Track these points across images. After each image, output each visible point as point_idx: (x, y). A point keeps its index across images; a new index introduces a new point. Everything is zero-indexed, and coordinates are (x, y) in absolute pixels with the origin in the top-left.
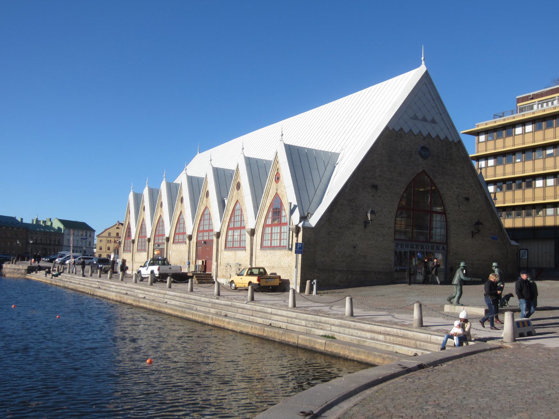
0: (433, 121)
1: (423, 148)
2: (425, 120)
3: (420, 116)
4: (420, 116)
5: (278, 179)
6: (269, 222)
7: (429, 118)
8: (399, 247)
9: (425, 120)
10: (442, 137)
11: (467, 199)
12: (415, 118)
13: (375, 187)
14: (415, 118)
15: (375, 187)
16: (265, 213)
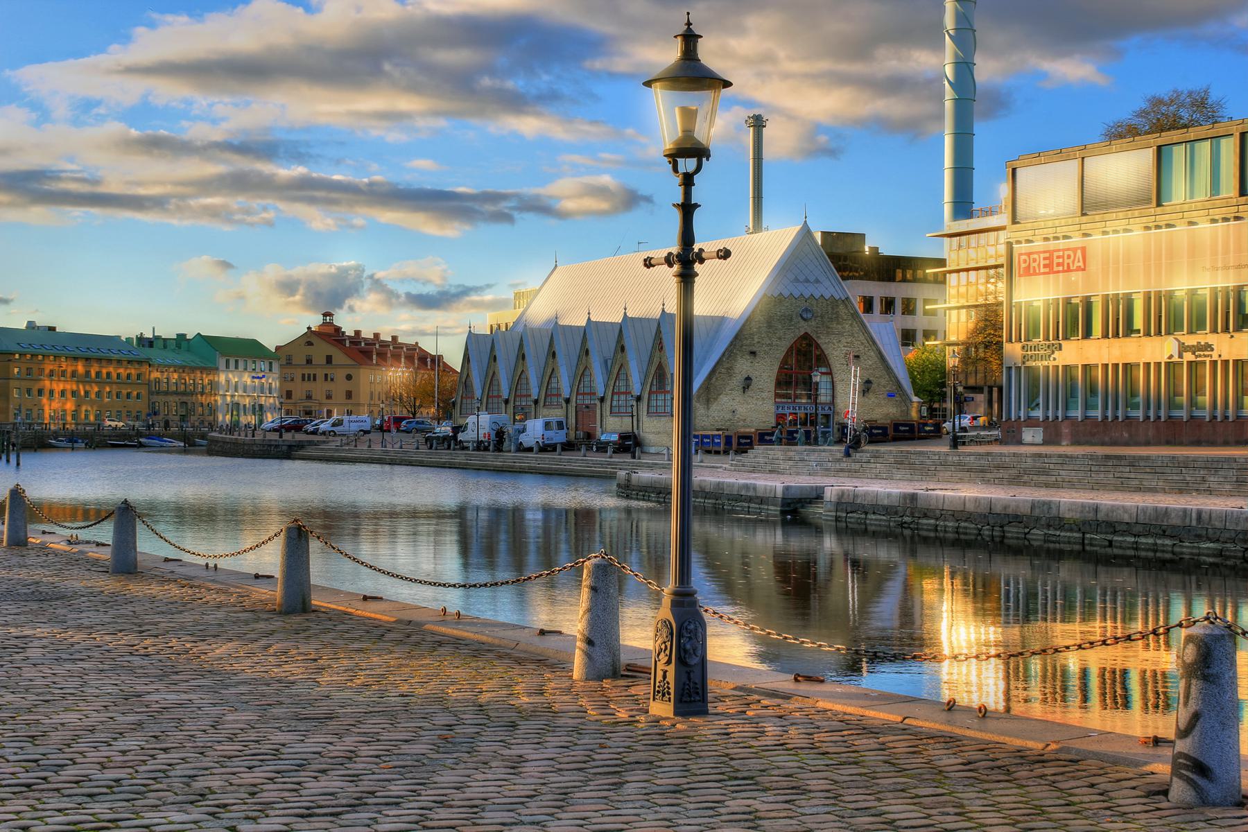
0: (817, 281)
1: (806, 310)
2: (807, 281)
3: (802, 278)
4: (802, 278)
5: (662, 348)
6: (654, 389)
7: (812, 279)
8: (780, 409)
9: (807, 281)
10: (827, 296)
11: (857, 357)
12: (797, 280)
13: (753, 353)
14: (797, 280)
15: (753, 353)
16: (650, 380)
